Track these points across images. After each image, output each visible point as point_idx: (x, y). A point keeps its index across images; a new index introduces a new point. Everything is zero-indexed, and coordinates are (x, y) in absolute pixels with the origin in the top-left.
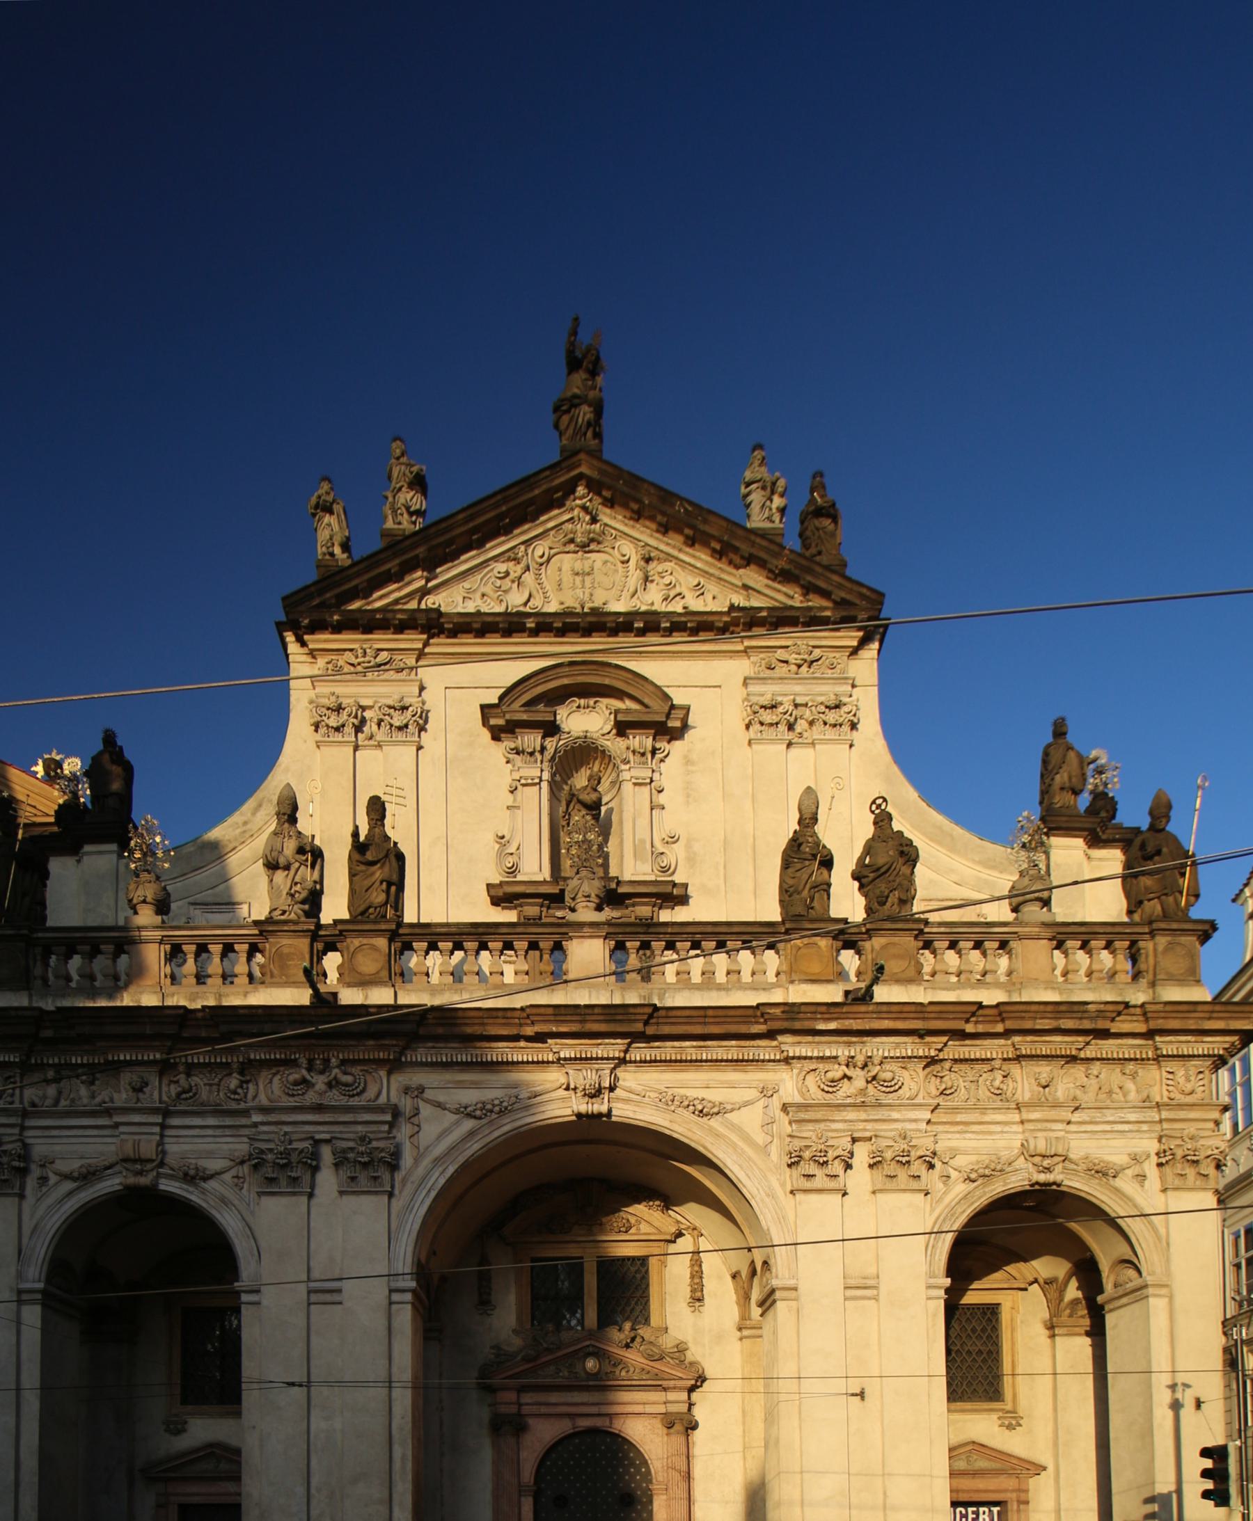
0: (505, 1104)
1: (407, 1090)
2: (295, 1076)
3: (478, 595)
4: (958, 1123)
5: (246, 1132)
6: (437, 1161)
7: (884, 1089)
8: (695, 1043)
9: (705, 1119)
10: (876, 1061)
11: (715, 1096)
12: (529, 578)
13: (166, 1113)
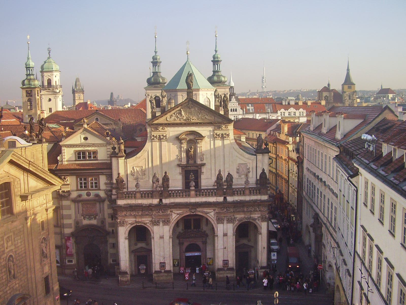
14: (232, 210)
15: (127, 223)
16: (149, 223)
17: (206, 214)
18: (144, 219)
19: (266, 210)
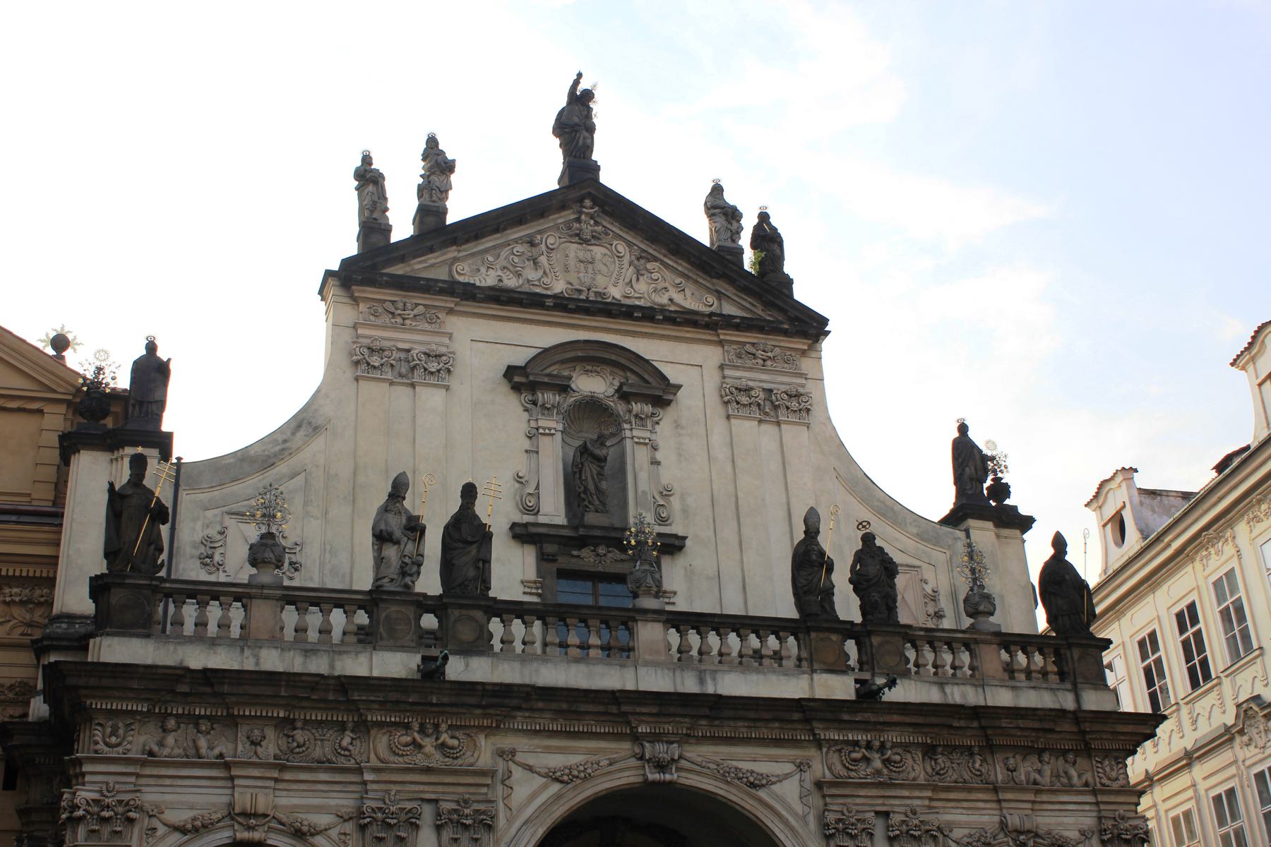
0: (589, 771)
1: (501, 753)
3: (498, 267)
7: (894, 769)
11: (763, 768)
13: (282, 768)
14: (917, 768)
15: (155, 823)
16: (334, 833)
17: (752, 785)
18: (295, 801)
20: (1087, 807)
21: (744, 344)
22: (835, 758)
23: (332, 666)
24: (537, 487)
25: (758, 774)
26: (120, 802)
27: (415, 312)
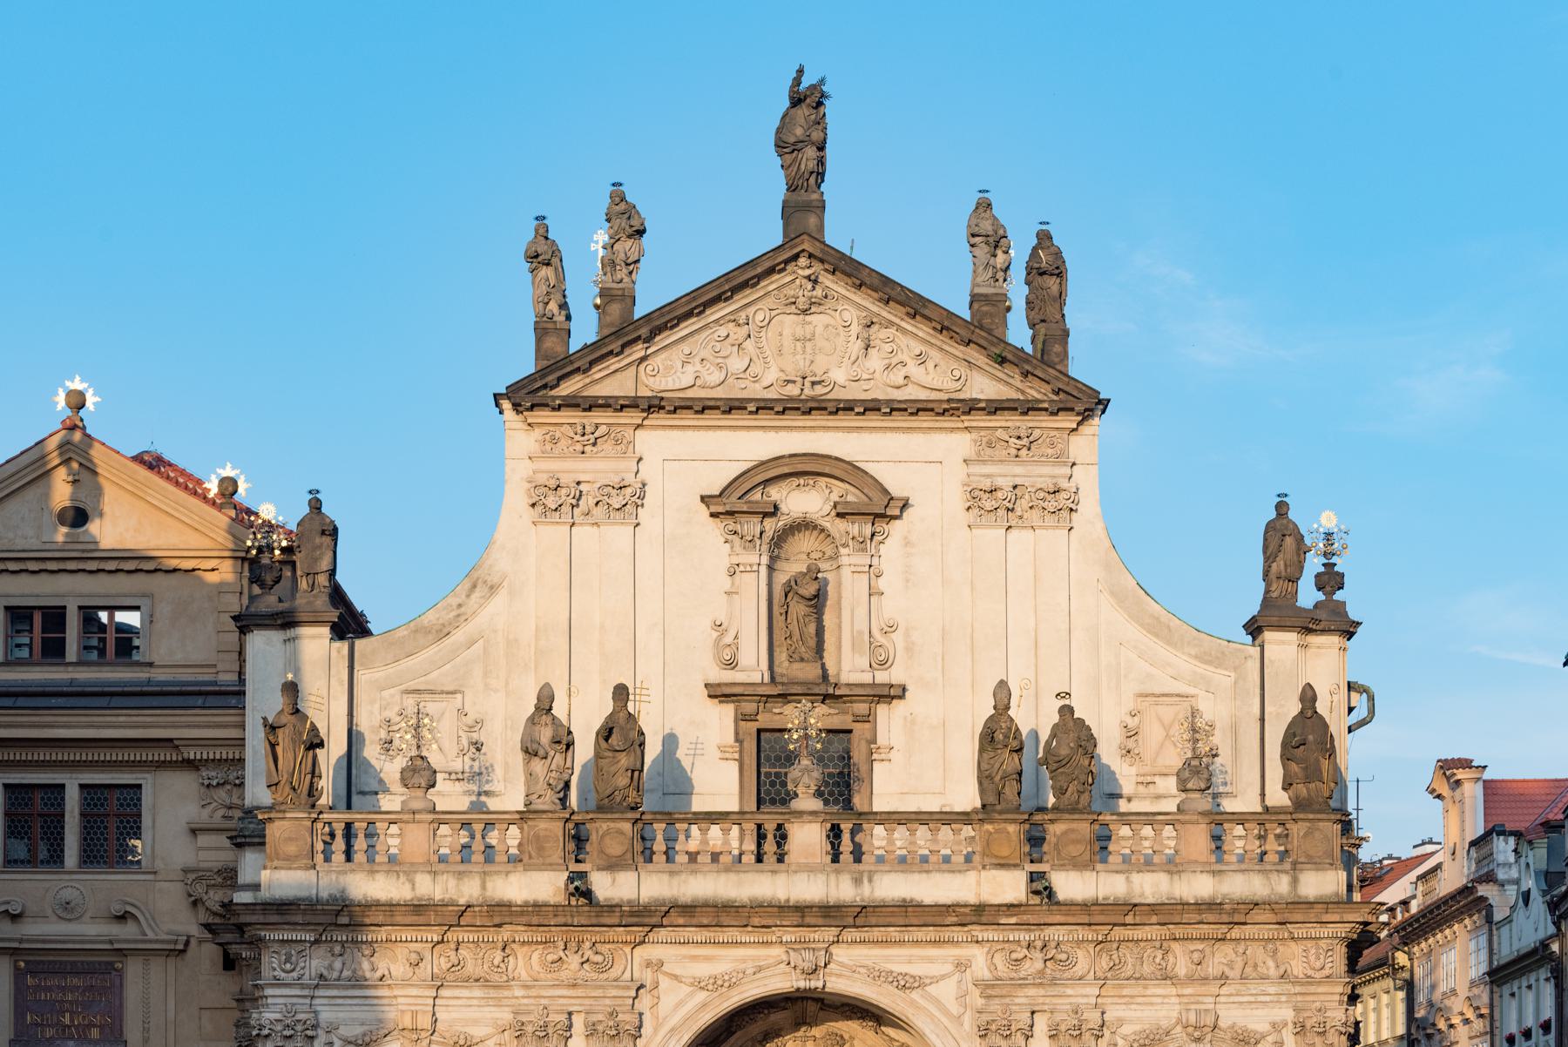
0: (734, 980)
1: (648, 964)
2: (550, 958)
3: (697, 360)
4: (1124, 996)
5: (505, 1002)
6: (672, 1030)
8: (898, 929)
9: (907, 991)
10: (1053, 944)
11: (916, 969)
12: (749, 344)
16: (490, 1043)
18: (454, 1015)
19: (1327, 972)
20: (1284, 998)
21: (996, 428)
22: (999, 959)
23: (484, 887)
24: (736, 637)
25: (912, 976)
26: (299, 1021)
27: (596, 435)
